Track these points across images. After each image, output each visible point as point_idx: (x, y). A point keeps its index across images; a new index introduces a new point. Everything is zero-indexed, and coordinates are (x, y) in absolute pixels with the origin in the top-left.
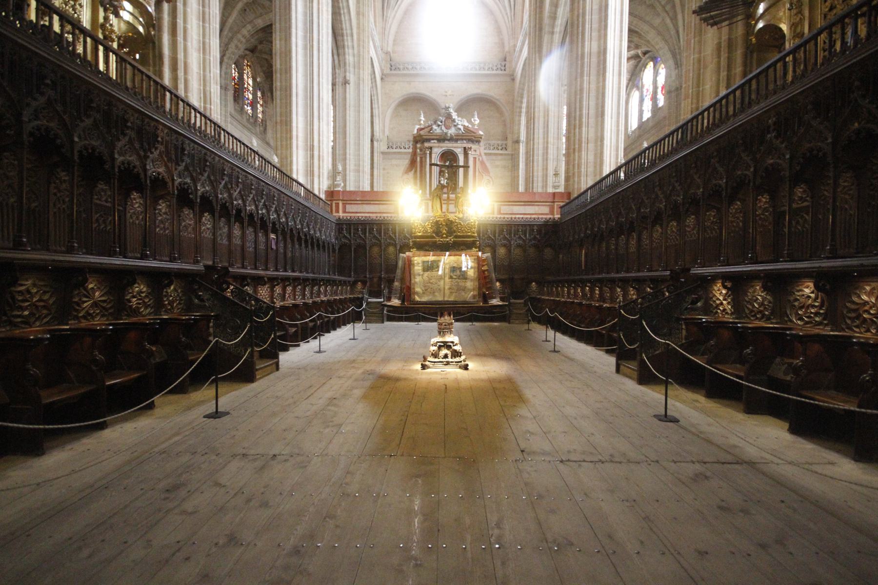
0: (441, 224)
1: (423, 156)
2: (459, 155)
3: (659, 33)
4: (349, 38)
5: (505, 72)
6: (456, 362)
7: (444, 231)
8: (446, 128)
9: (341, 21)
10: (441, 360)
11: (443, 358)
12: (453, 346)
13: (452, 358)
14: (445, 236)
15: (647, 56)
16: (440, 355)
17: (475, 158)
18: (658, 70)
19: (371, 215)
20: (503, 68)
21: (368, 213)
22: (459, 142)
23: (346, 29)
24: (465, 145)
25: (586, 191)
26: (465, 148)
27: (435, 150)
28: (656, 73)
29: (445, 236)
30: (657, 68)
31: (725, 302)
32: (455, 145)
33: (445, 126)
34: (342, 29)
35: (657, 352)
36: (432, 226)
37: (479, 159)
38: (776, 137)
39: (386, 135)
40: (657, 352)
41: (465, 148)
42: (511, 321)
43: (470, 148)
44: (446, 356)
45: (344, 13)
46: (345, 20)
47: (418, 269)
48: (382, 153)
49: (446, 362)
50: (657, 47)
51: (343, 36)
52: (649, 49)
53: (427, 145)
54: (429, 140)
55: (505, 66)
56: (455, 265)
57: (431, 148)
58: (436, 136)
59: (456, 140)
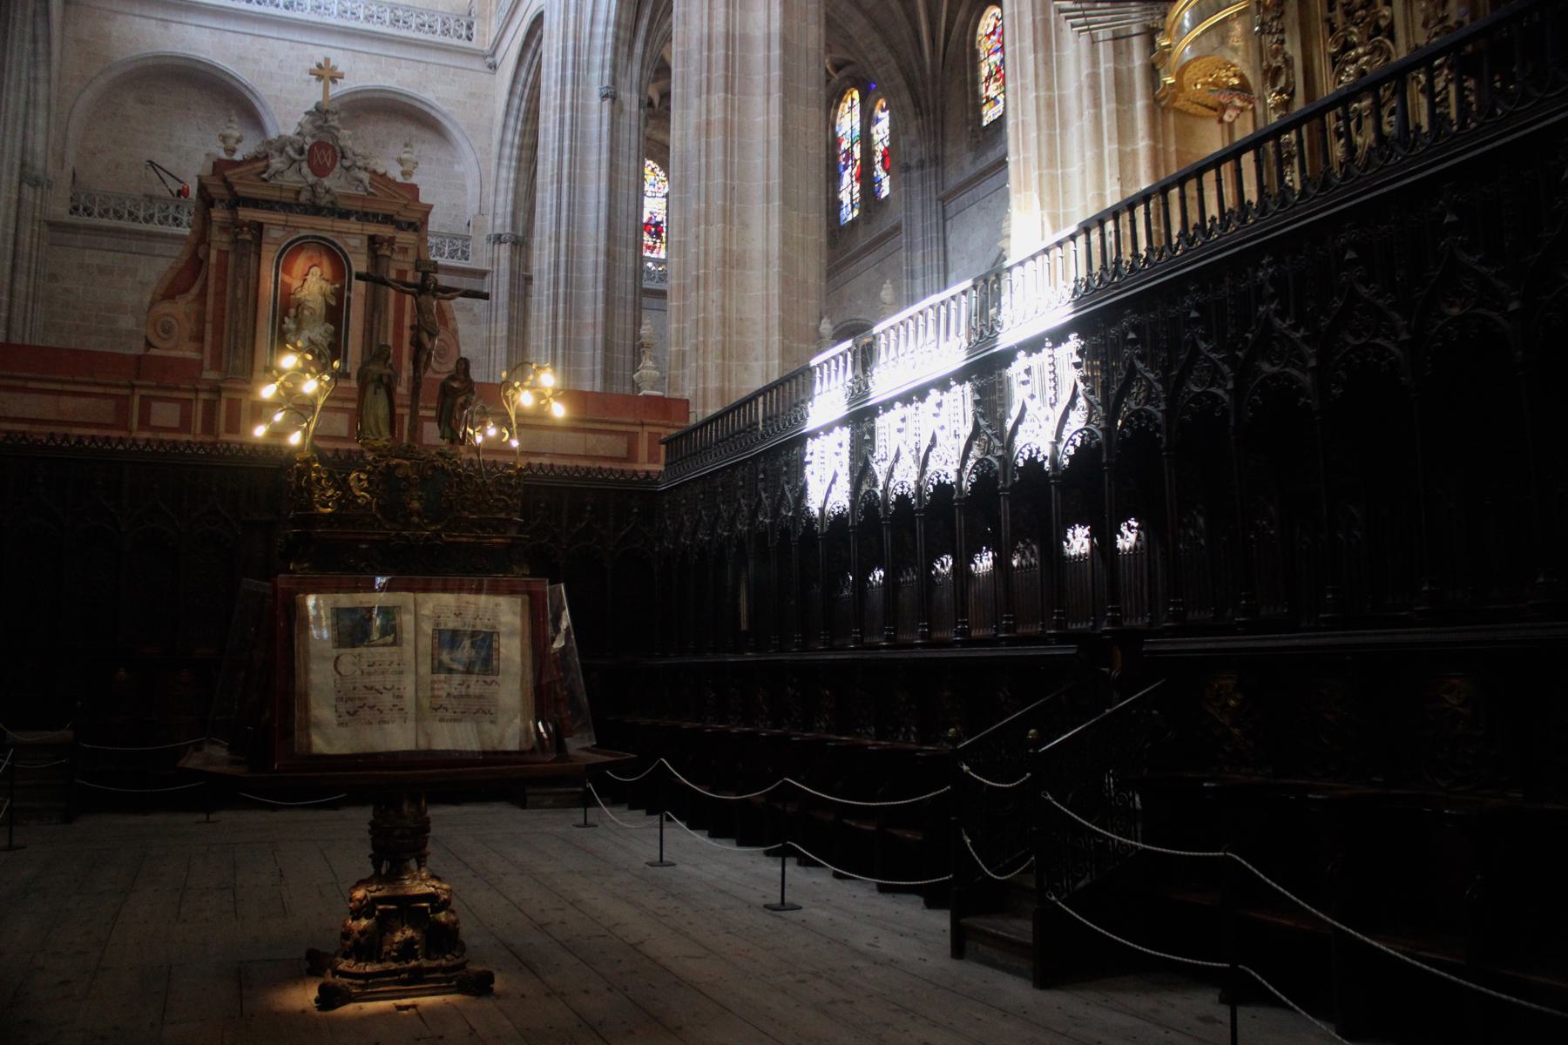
0: (406, 478)
2: (350, 257)
3: (877, 27)
5: (466, 44)
6: (445, 970)
7: (416, 505)
8: (315, 172)
10: (393, 966)
11: (395, 960)
12: (436, 910)
13: (428, 957)
14: (416, 519)
15: (843, 73)
16: (386, 948)
18: (872, 111)
19: (36, 429)
20: (464, 33)
21: (16, 420)
22: (353, 219)
25: (752, 398)
26: (372, 239)
28: (868, 120)
29: (416, 519)
30: (870, 105)
31: (1236, 731)
32: (342, 225)
33: (310, 166)
35: (1081, 884)
36: (370, 482)
38: (1282, 314)
39: (68, 169)
40: (1081, 884)
41: (372, 239)
42: (529, 799)
43: (391, 241)
44: (407, 950)
47: (321, 633)
48: (55, 226)
49: (412, 970)
50: (872, 57)
52: (852, 59)
53: (245, 214)
54: (255, 203)
55: (469, 27)
56: (452, 624)
57: (259, 228)
59: (345, 215)
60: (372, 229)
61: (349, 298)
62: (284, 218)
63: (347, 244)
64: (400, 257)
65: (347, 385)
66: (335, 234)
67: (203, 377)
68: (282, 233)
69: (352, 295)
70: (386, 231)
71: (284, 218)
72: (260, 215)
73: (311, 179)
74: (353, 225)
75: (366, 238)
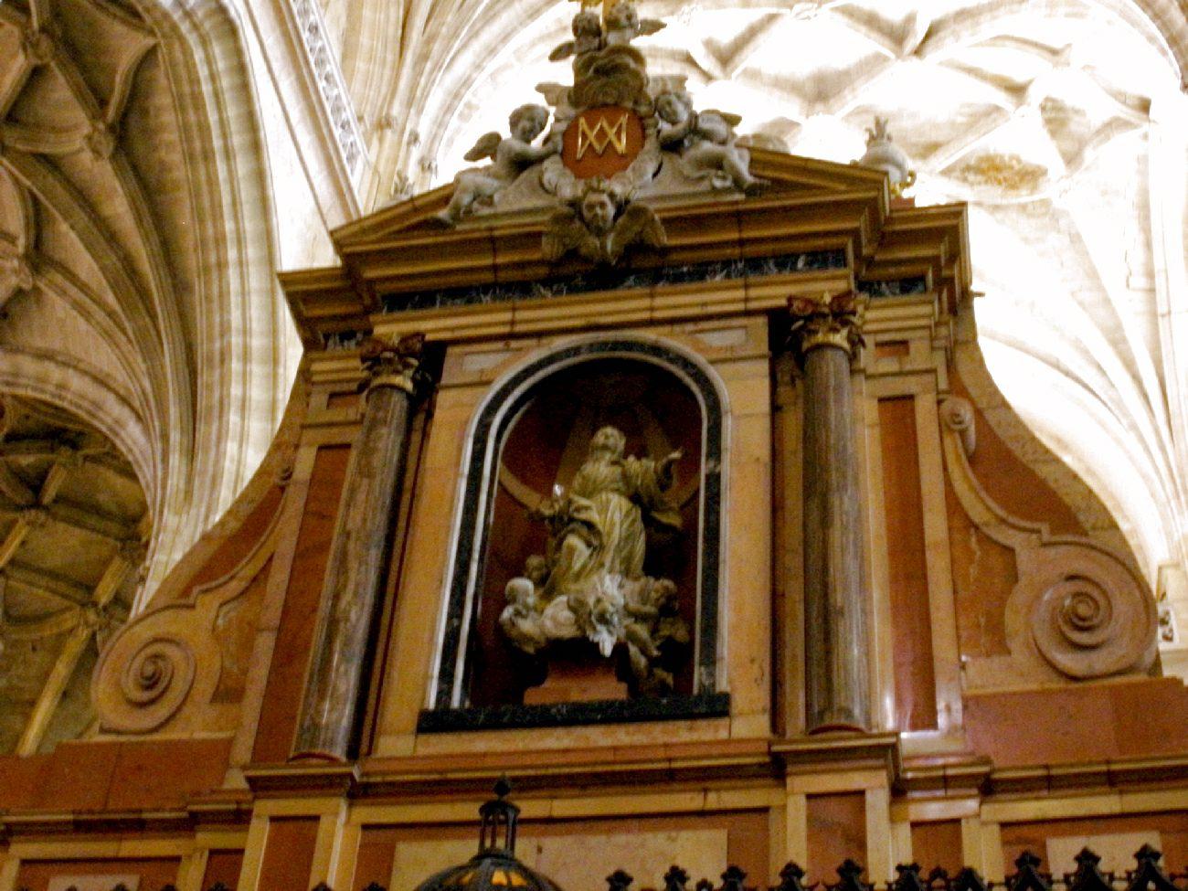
1: (354, 436)
2: (713, 373)
4: (257, 370)
9: (223, 295)
17: (898, 407)
23: (245, 332)
24: (774, 292)
26: (779, 320)
27: (461, 366)
34: (225, 330)
37: (949, 425)
41: (779, 320)
45: (241, 263)
46: (244, 294)
51: (224, 357)
53: (390, 329)
57: (431, 358)
58: (492, 243)
60: (774, 292)
61: (714, 479)
62: (507, 316)
63: (703, 350)
64: (889, 365)
65: (723, 735)
66: (667, 329)
67: (226, 786)
68: (500, 358)
69: (726, 468)
70: (825, 287)
71: (507, 316)
72: (434, 325)
73: (569, 187)
74: (720, 295)
75: (761, 323)
